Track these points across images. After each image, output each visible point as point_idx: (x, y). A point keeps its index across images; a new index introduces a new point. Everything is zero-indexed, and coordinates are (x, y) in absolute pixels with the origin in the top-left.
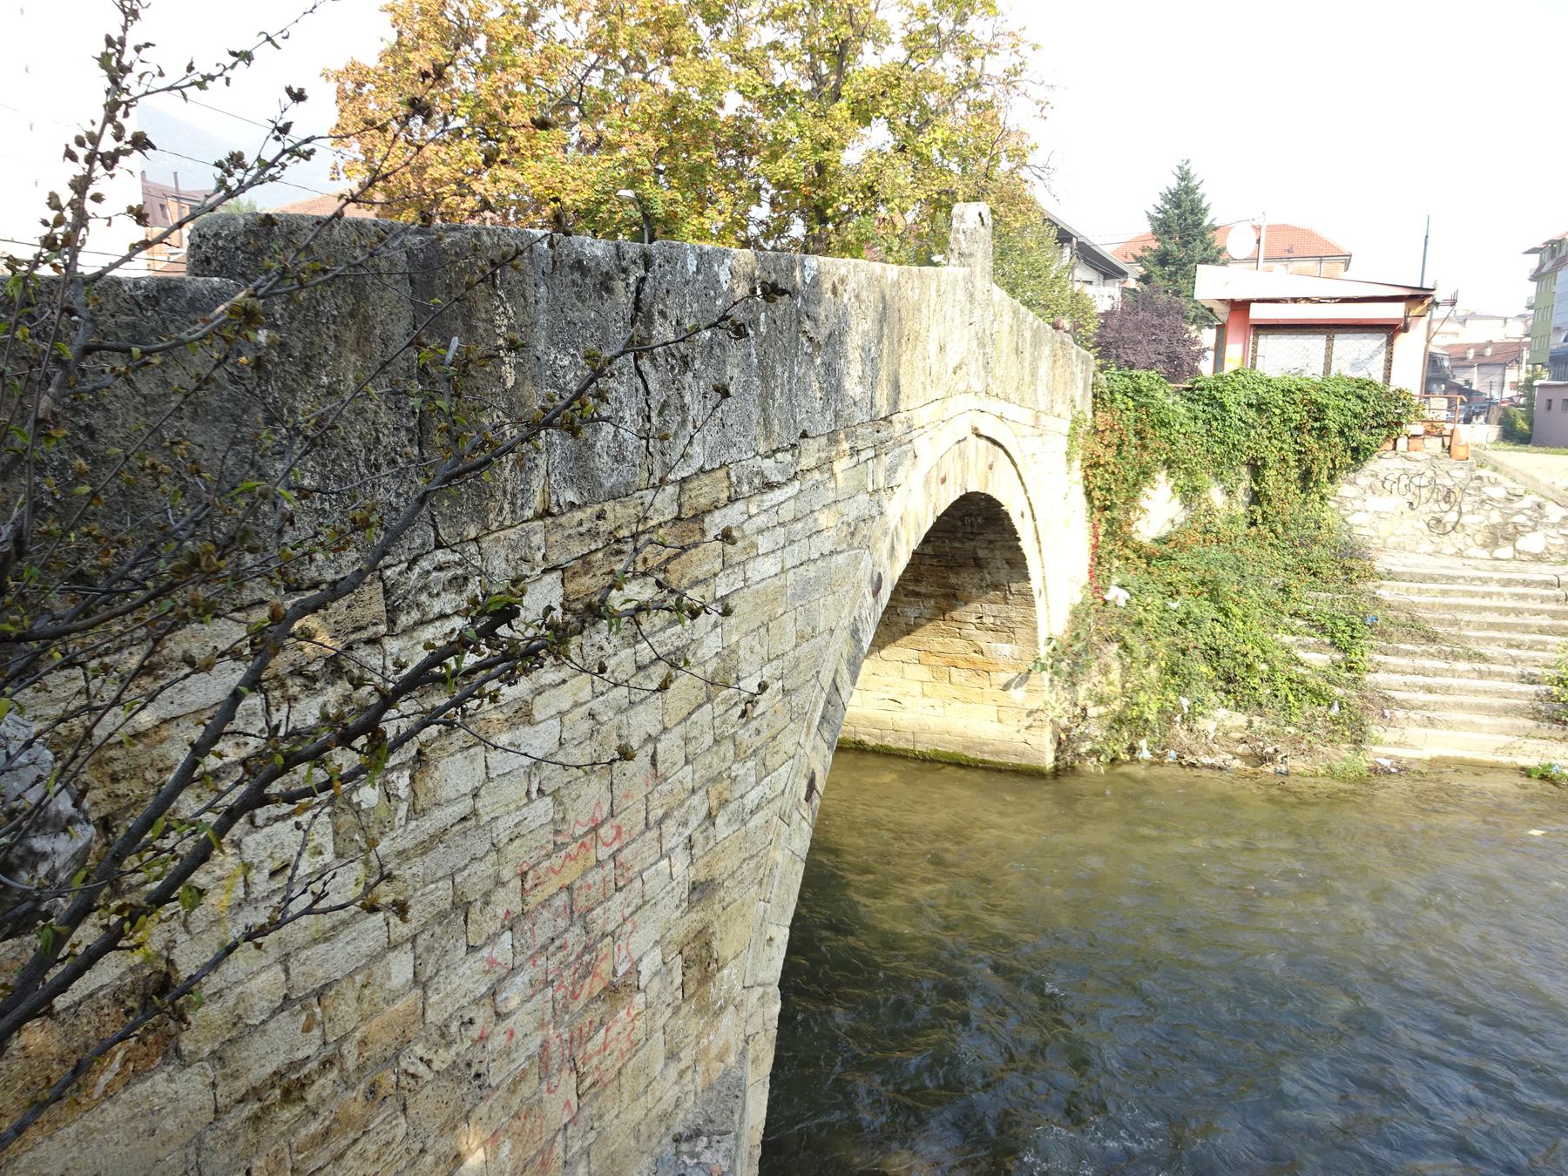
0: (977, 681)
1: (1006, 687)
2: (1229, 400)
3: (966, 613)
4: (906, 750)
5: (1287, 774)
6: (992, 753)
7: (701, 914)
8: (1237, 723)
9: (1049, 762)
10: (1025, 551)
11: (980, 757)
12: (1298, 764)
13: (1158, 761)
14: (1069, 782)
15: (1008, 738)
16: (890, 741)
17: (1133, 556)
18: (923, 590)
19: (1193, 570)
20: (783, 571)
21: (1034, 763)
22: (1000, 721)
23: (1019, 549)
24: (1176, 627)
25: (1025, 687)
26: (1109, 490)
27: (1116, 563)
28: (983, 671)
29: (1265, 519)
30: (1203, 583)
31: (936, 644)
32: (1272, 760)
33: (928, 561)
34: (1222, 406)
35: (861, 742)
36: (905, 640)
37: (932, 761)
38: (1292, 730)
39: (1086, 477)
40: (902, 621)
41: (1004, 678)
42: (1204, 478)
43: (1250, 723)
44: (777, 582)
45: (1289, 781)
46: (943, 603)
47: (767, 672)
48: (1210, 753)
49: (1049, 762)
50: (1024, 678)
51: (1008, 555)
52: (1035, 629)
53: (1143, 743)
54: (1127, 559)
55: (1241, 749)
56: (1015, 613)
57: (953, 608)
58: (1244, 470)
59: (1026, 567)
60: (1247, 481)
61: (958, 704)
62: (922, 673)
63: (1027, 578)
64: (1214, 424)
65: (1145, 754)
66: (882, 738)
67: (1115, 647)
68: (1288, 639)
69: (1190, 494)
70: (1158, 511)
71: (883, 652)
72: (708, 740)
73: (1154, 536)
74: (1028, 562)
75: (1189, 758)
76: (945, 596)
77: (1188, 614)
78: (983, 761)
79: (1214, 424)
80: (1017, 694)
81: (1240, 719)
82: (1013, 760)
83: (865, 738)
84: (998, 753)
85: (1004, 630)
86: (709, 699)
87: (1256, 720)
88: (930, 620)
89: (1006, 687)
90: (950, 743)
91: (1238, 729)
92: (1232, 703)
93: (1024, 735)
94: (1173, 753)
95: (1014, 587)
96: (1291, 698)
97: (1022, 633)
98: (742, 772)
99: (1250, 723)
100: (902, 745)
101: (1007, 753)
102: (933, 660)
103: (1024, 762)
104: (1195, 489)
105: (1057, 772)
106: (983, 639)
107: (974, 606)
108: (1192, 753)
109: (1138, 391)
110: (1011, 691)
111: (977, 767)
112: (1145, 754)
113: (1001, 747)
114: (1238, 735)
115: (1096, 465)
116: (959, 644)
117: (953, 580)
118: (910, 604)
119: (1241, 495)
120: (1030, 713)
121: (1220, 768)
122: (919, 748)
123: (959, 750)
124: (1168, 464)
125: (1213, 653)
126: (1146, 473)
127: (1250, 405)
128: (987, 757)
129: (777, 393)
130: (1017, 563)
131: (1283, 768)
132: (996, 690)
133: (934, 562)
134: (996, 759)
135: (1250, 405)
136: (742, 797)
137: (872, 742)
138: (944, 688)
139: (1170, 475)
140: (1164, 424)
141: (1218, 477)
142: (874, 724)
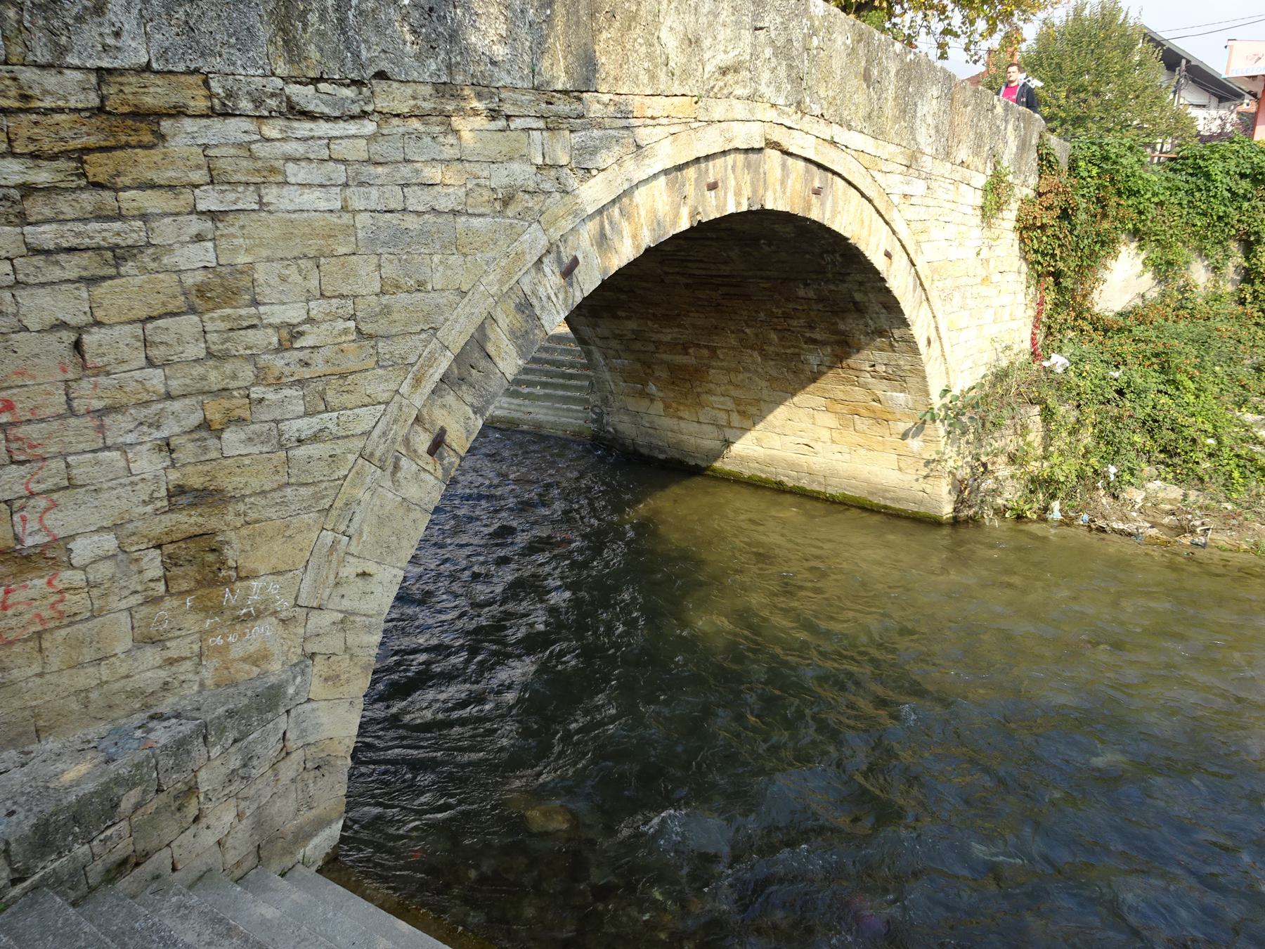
0: (877, 428)
1: (904, 436)
2: (1216, 169)
3: (861, 360)
4: (819, 493)
5: (1204, 546)
6: (892, 499)
7: (200, 520)
8: (1172, 496)
9: (947, 511)
10: (897, 293)
11: (883, 502)
12: (1223, 539)
13: (1067, 522)
14: (965, 533)
15: (907, 486)
16: (805, 483)
17: (1087, 327)
18: (817, 336)
19: (1146, 342)
20: (344, 209)
21: (932, 512)
22: (900, 469)
23: (888, 291)
24: (1111, 395)
25: (921, 437)
26: (1053, 256)
27: (1071, 334)
28: (881, 419)
29: (1256, 298)
30: (1157, 355)
31: (839, 391)
32: (1193, 532)
33: (815, 307)
34: (1208, 176)
35: (780, 483)
36: (812, 387)
37: (840, 503)
38: (1229, 506)
39: (1022, 240)
40: (807, 368)
41: (902, 427)
42: (1181, 251)
43: (1185, 496)
44: (333, 218)
45: (1200, 553)
46: (839, 350)
47: (317, 308)
48: (1125, 518)
49: (947, 511)
50: (920, 428)
51: (882, 299)
52: (924, 378)
53: (1056, 505)
54: (1082, 331)
55: (1166, 520)
56: (904, 361)
57: (848, 355)
58: (1234, 246)
59: (901, 312)
60: (1238, 258)
61: (862, 451)
62: (828, 420)
63: (905, 323)
64: (1197, 195)
65: (1056, 515)
66: (799, 479)
67: (1038, 408)
68: (1249, 417)
69: (1164, 269)
70: (1123, 281)
71: (795, 399)
72: (198, 350)
73: (1118, 309)
74: (902, 306)
75: (1101, 523)
76: (839, 343)
77: (1128, 383)
78: (885, 507)
79: (1197, 195)
80: (915, 444)
81: (1175, 492)
82: (912, 507)
83: (784, 479)
84: (898, 500)
85: (895, 378)
86: (193, 310)
87: (1193, 495)
88: (830, 368)
89: (904, 436)
90: (856, 487)
91: (1170, 502)
92: (1170, 476)
93: (922, 484)
94: (1086, 517)
95: (897, 333)
96: (1236, 474)
97: (913, 381)
98: (271, 396)
99: (1185, 496)
100: (815, 487)
101: (907, 500)
102: (838, 407)
103: (922, 510)
104: (1170, 263)
105: (955, 522)
106: (880, 388)
107: (865, 353)
108: (1104, 518)
109: (1106, 158)
110: (909, 441)
111: (879, 512)
112: (1056, 515)
113: (902, 494)
114: (1168, 507)
115: (1033, 227)
116: (859, 393)
117: (842, 327)
118: (811, 351)
119: (1230, 270)
120: (928, 463)
121: (1130, 535)
122: (830, 491)
123: (864, 495)
124: (1136, 233)
125: (1151, 425)
126: (1106, 243)
127: (1243, 176)
128: (889, 503)
129: (313, 18)
130: (891, 306)
131: (1203, 540)
132: (895, 439)
133: (820, 307)
134: (897, 506)
135: (1243, 176)
136: (277, 422)
137: (790, 483)
138: (850, 436)
139: (1141, 248)
140: (1134, 193)
141: (1201, 251)
142: (792, 466)
